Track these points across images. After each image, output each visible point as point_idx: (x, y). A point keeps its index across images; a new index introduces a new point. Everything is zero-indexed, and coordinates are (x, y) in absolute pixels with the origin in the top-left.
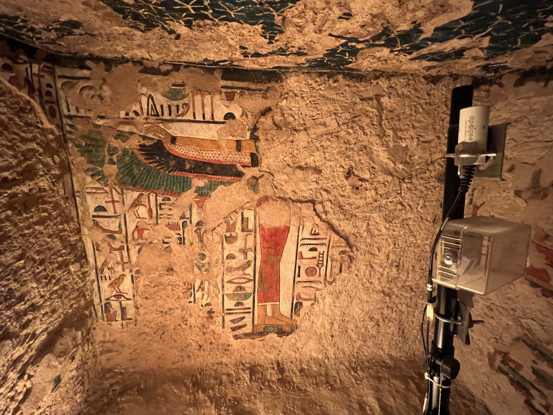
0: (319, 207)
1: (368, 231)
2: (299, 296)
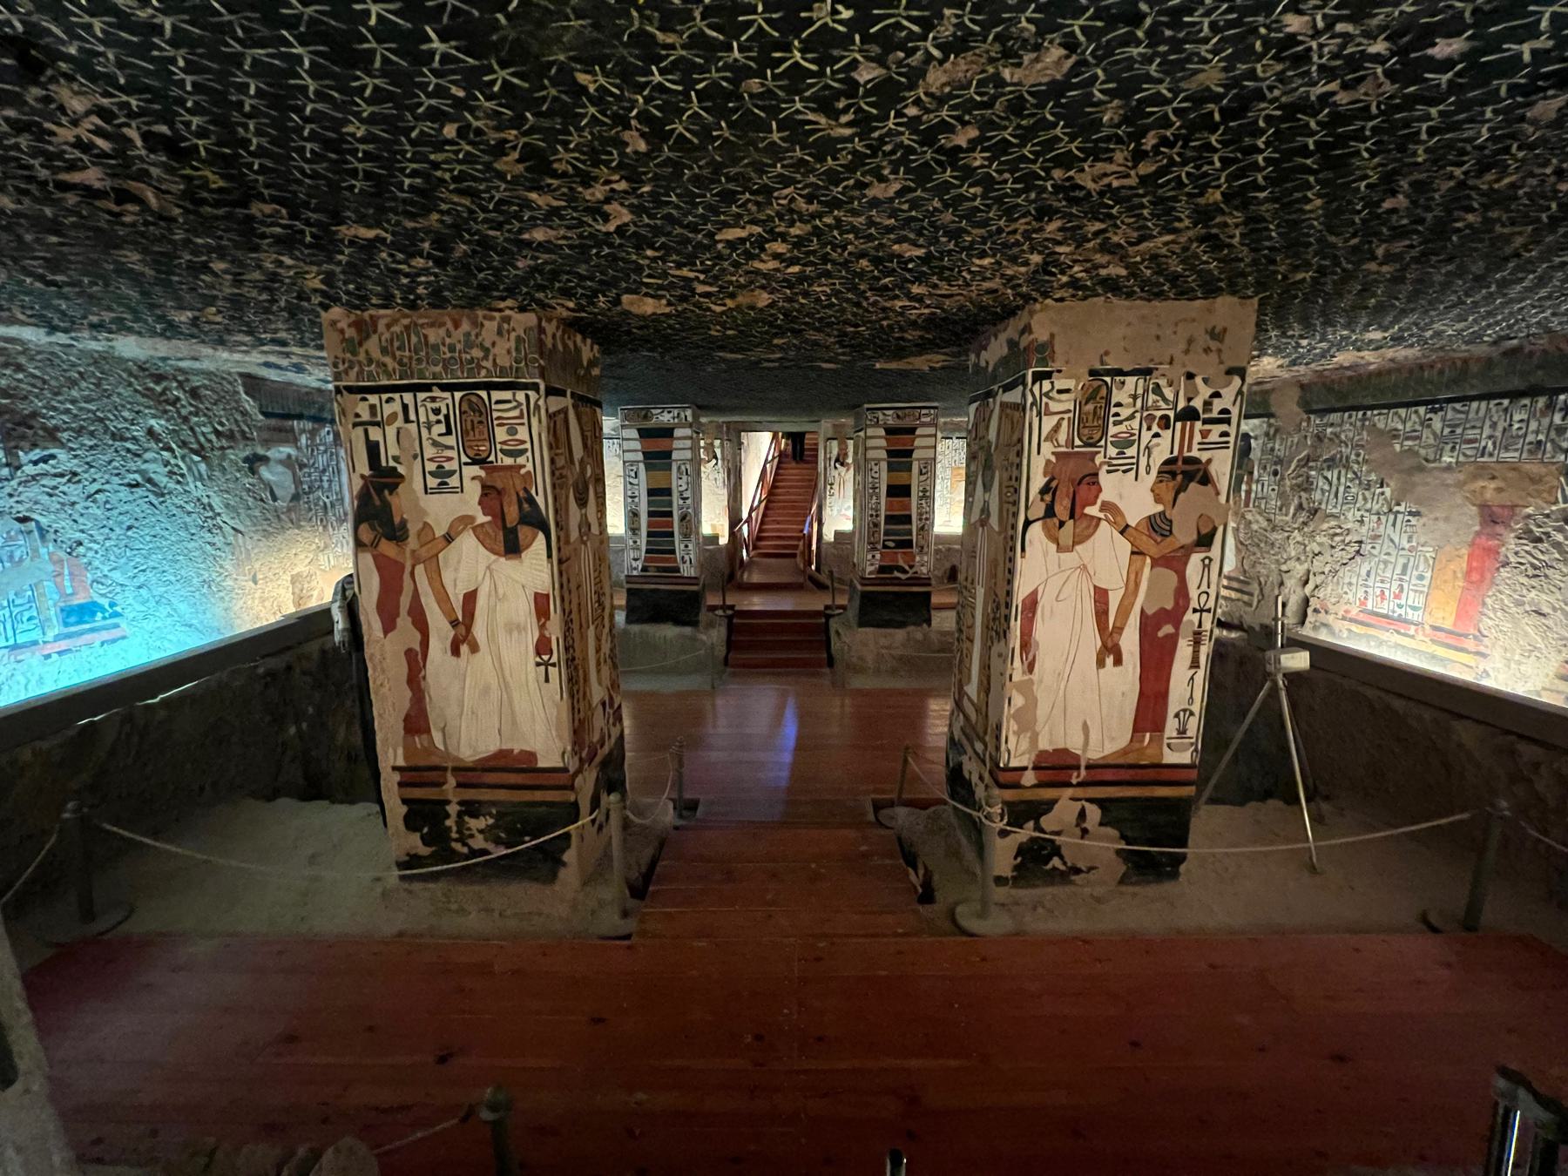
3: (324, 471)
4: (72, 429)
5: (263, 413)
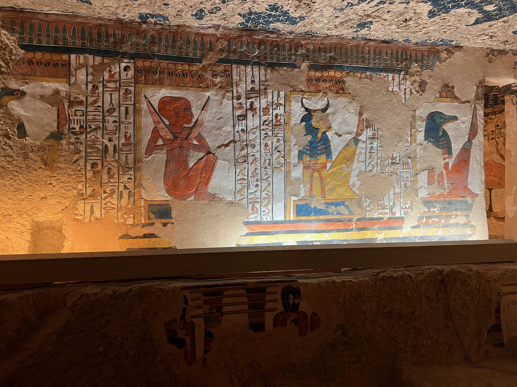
3: (111, 111)
5: (23, 47)
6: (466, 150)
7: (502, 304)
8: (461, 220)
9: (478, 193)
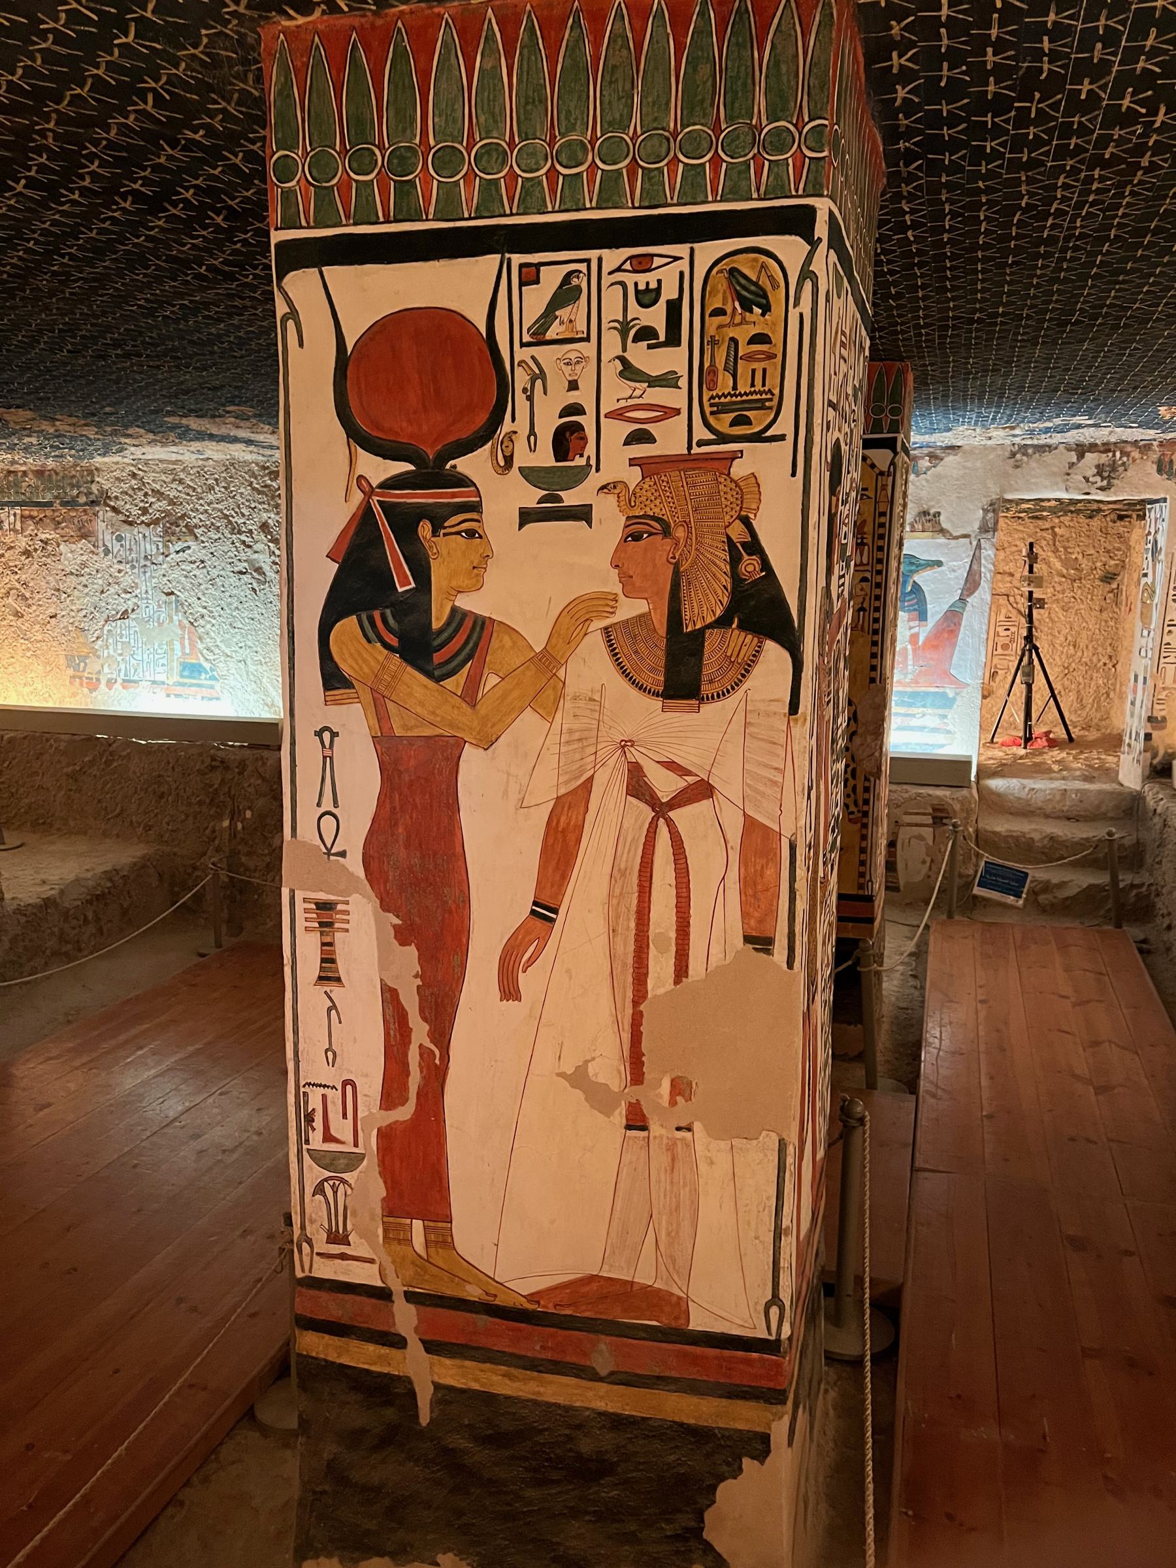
0: (1011, 599)
1: (1050, 618)
2: (996, 667)
4: (205, 526)
6: (953, 617)
7: (900, 836)
8: (932, 721)
9: (969, 681)
